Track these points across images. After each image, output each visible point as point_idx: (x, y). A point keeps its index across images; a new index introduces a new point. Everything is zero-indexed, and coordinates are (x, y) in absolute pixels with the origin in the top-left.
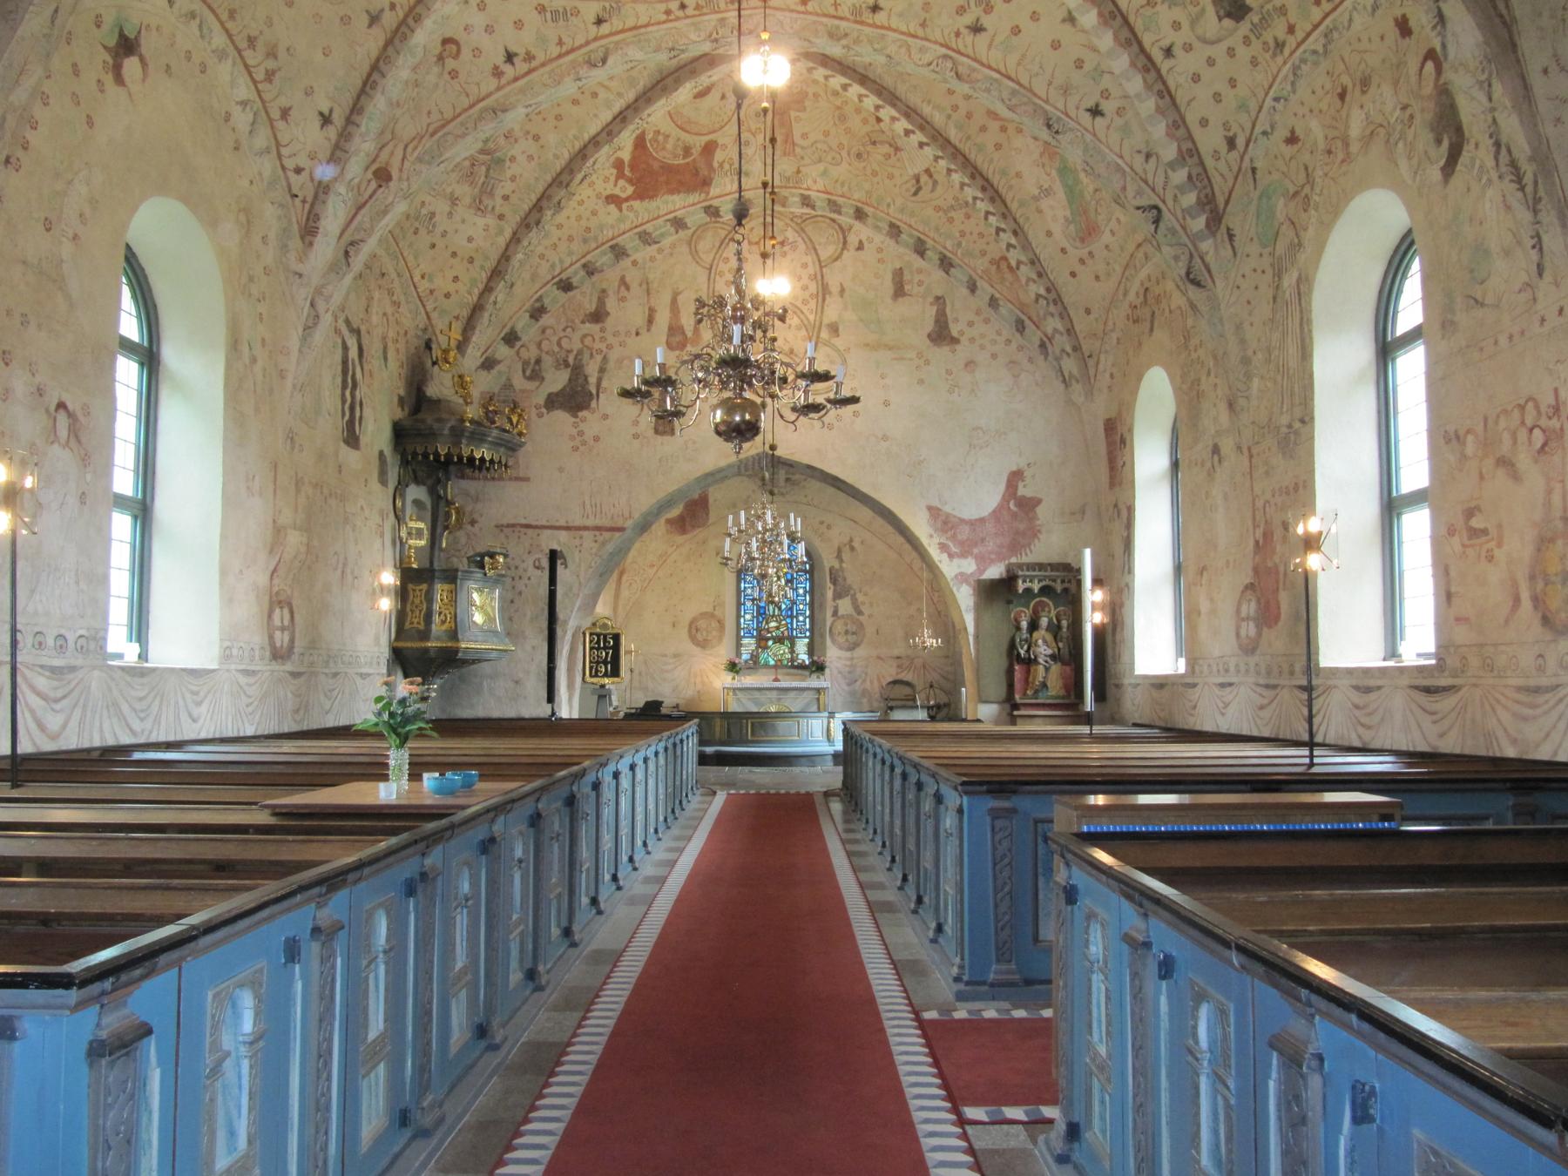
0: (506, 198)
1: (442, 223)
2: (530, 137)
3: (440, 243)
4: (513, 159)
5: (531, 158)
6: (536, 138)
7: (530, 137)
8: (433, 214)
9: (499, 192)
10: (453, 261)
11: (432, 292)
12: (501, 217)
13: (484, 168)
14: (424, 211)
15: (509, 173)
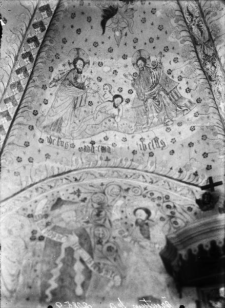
0: (188, 90)
1: (167, 138)
2: (164, 53)
3: (175, 147)
4: (170, 72)
5: (176, 60)
6: (166, 49)
7: (164, 53)
8: (156, 140)
9: (182, 92)
10: (193, 149)
11: (196, 174)
12: (199, 101)
13: (162, 93)
14: (146, 142)
15: (176, 80)
